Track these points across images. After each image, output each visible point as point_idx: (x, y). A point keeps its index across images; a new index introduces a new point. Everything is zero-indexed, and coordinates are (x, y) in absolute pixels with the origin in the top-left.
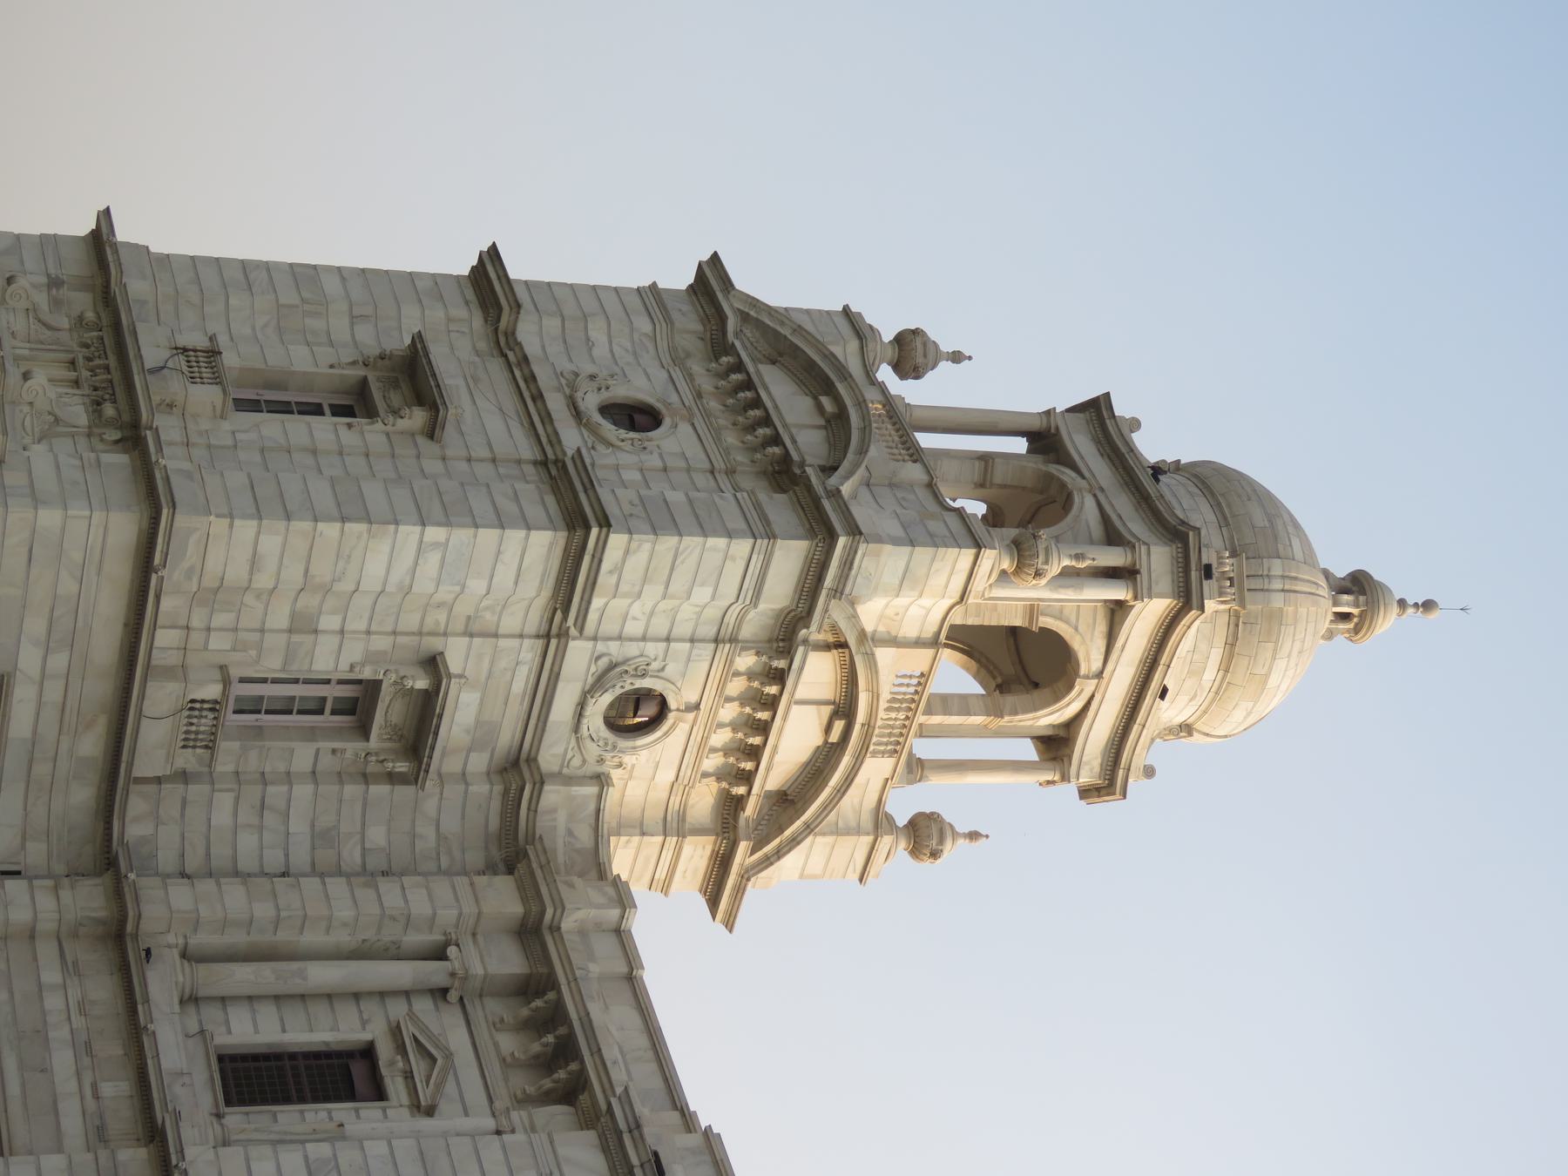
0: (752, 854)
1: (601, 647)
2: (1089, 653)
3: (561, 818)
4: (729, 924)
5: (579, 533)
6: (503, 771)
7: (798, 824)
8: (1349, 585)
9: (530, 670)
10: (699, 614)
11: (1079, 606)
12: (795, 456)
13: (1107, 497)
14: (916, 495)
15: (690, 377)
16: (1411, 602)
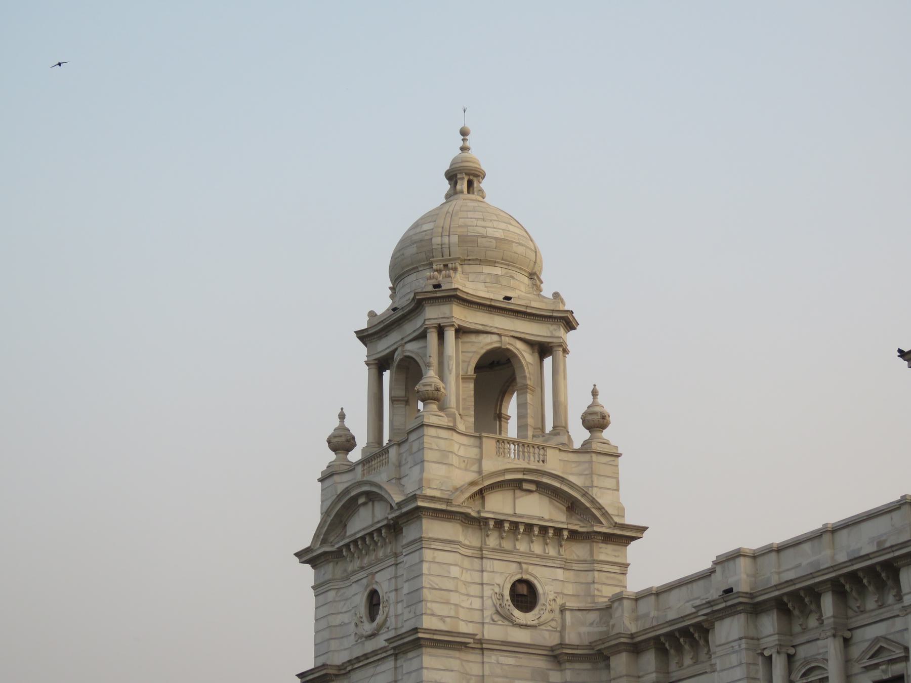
0: (602, 523)
1: (487, 620)
2: (487, 343)
3: (584, 630)
4: (643, 529)
5: (422, 642)
6: (559, 663)
7: (583, 500)
8: (453, 182)
9: (501, 656)
10: (467, 570)
11: (462, 352)
12: (385, 522)
13: (406, 337)
14: (404, 452)
15: (354, 572)
16: (461, 144)
